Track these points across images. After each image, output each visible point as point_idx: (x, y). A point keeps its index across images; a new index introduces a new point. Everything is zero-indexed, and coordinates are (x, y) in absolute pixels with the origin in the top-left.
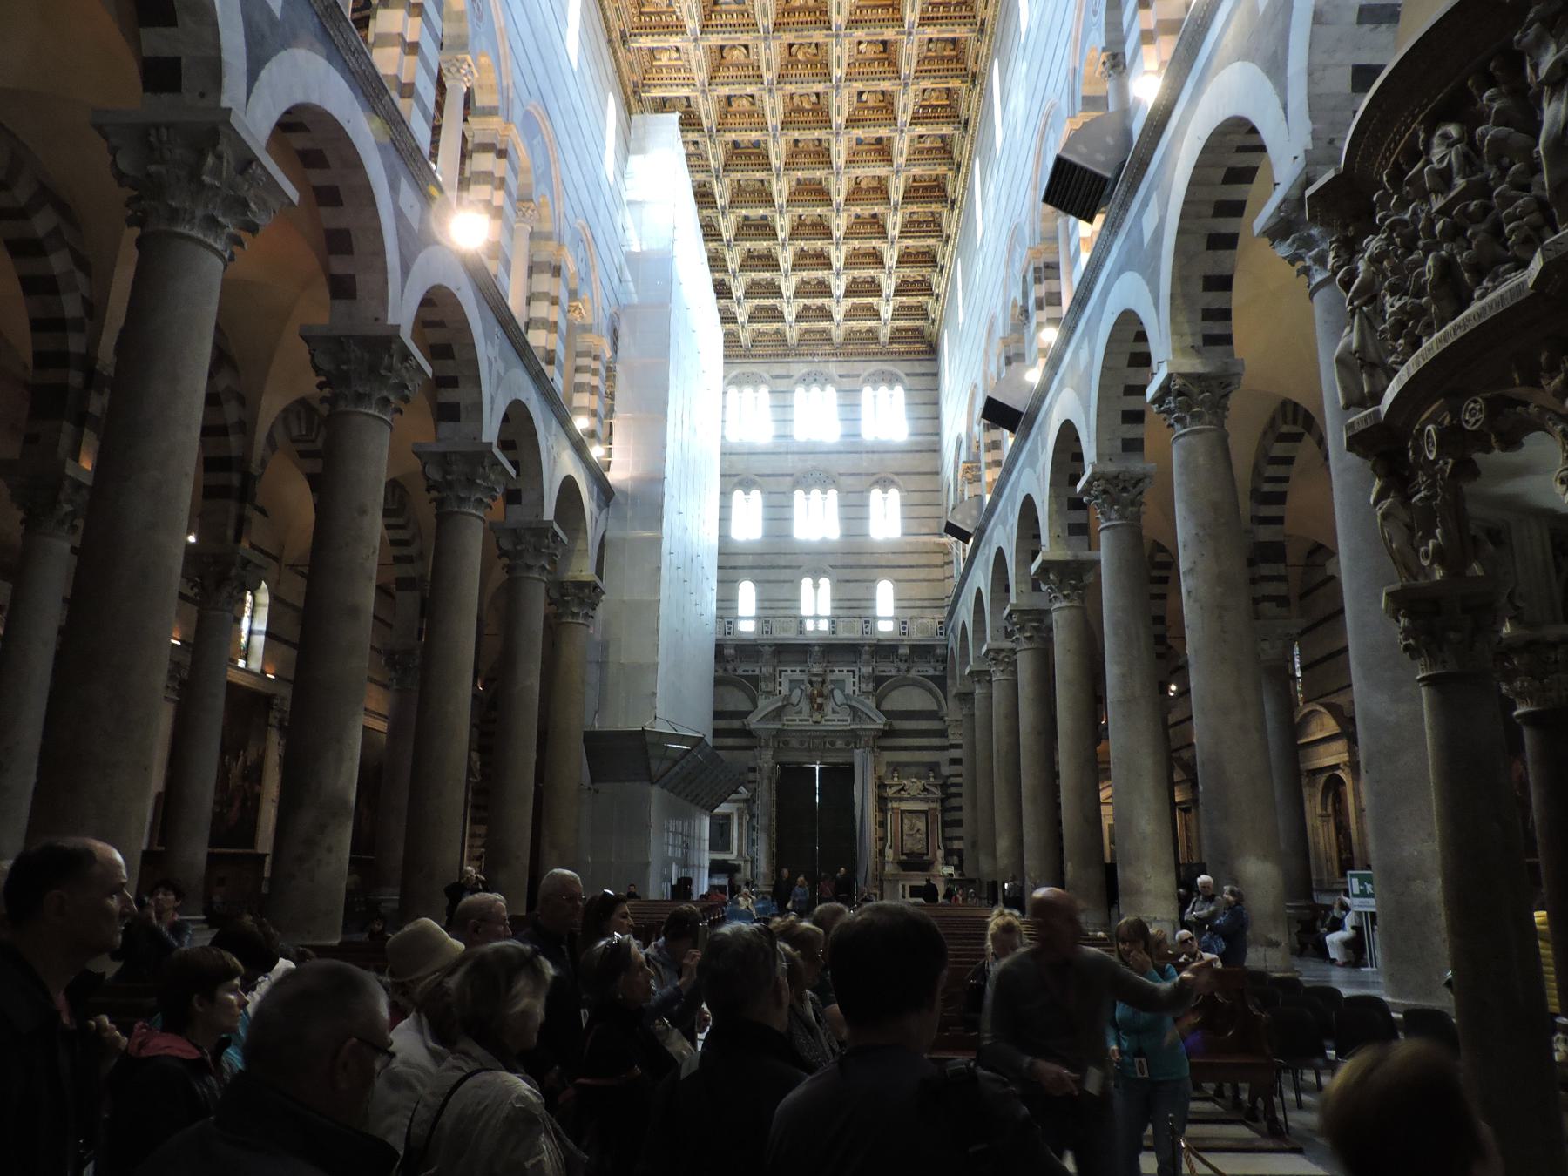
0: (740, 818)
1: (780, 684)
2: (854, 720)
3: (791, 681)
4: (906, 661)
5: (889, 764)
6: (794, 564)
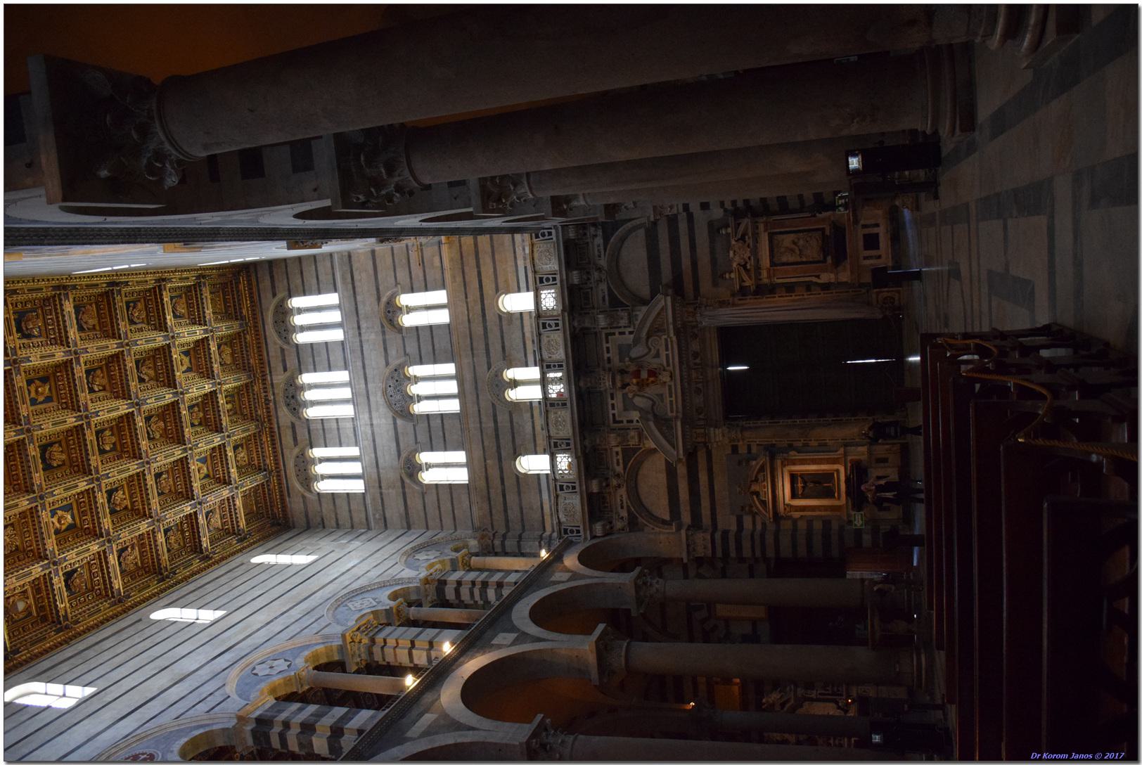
0: (794, 463)
3: (626, 409)
4: (588, 273)
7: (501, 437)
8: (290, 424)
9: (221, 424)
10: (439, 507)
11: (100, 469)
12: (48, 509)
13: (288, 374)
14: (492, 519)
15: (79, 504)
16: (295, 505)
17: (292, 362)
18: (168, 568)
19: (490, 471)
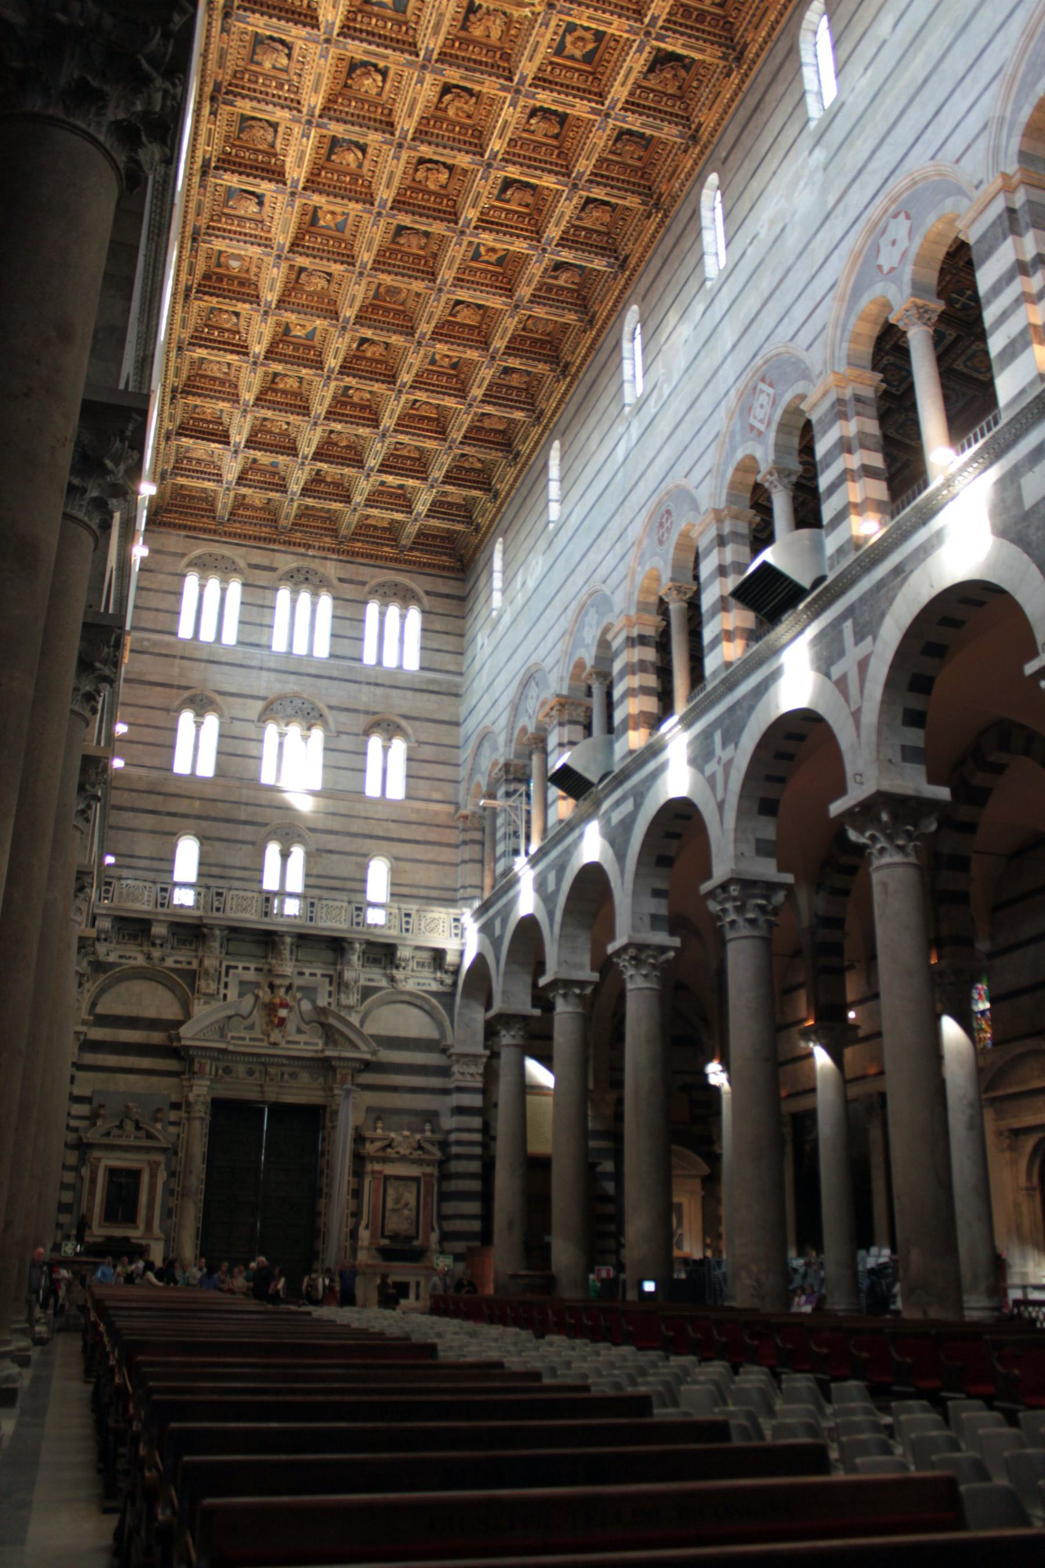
1: (226, 986)
2: (326, 1044)
3: (242, 983)
5: (369, 1110)
6: (259, 820)
19: (187, 801)
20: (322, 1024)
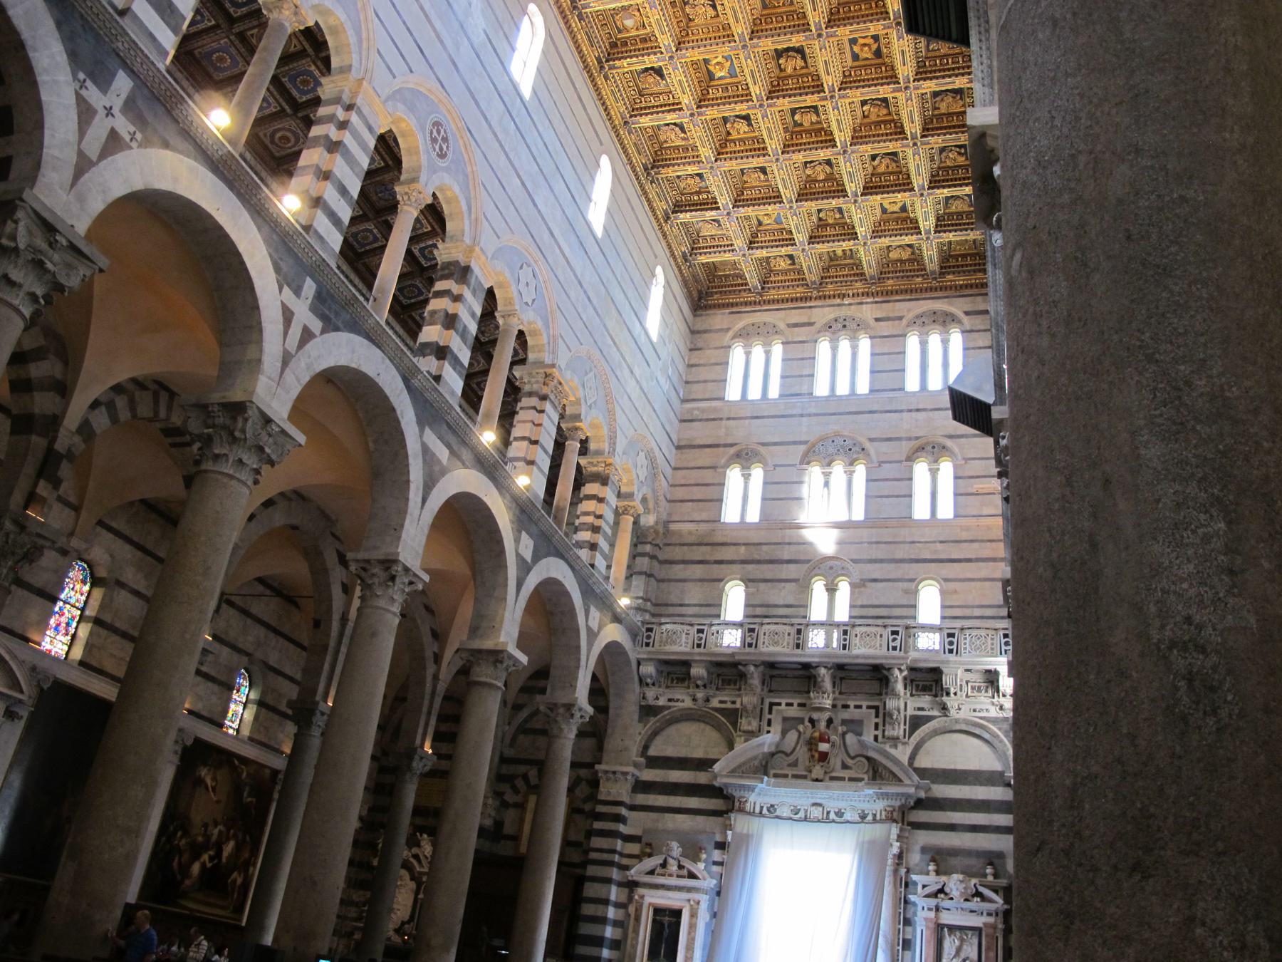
3: (785, 719)
6: (802, 558)
7: (771, 566)
8: (812, 321)
9: (818, 243)
10: (698, 485)
11: (772, 109)
12: (731, 54)
13: (872, 323)
14: (676, 545)
15: (736, 84)
16: (719, 319)
17: (885, 328)
18: (659, 176)
20: (868, 759)
